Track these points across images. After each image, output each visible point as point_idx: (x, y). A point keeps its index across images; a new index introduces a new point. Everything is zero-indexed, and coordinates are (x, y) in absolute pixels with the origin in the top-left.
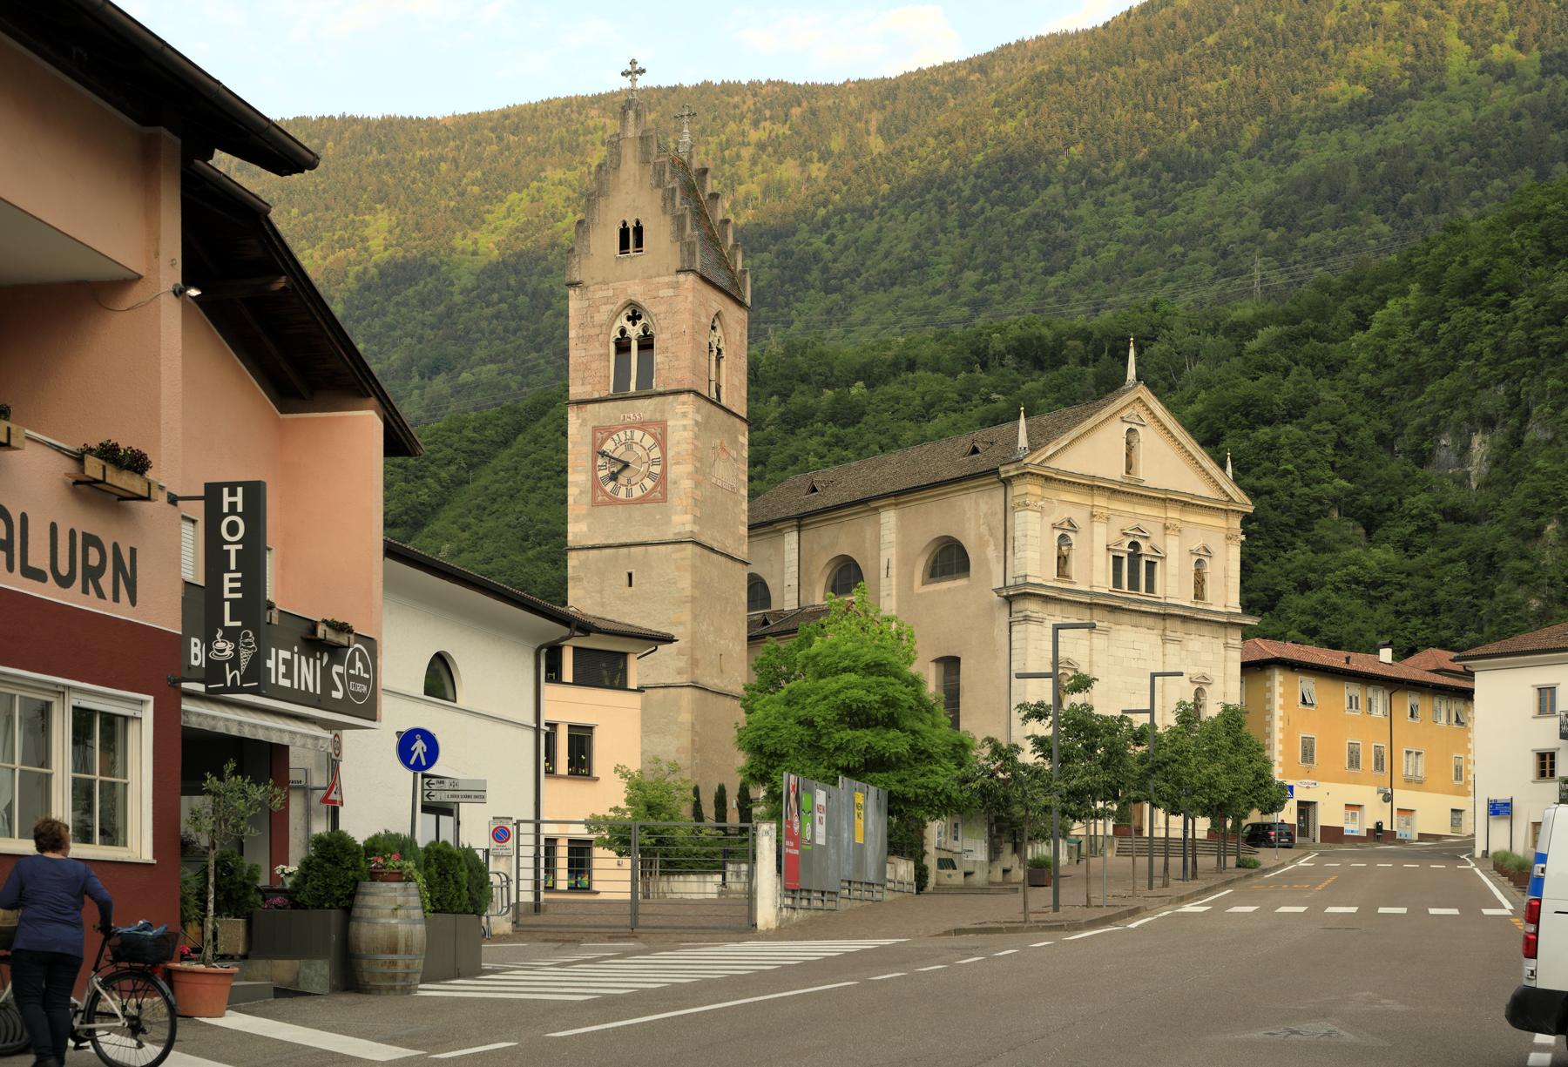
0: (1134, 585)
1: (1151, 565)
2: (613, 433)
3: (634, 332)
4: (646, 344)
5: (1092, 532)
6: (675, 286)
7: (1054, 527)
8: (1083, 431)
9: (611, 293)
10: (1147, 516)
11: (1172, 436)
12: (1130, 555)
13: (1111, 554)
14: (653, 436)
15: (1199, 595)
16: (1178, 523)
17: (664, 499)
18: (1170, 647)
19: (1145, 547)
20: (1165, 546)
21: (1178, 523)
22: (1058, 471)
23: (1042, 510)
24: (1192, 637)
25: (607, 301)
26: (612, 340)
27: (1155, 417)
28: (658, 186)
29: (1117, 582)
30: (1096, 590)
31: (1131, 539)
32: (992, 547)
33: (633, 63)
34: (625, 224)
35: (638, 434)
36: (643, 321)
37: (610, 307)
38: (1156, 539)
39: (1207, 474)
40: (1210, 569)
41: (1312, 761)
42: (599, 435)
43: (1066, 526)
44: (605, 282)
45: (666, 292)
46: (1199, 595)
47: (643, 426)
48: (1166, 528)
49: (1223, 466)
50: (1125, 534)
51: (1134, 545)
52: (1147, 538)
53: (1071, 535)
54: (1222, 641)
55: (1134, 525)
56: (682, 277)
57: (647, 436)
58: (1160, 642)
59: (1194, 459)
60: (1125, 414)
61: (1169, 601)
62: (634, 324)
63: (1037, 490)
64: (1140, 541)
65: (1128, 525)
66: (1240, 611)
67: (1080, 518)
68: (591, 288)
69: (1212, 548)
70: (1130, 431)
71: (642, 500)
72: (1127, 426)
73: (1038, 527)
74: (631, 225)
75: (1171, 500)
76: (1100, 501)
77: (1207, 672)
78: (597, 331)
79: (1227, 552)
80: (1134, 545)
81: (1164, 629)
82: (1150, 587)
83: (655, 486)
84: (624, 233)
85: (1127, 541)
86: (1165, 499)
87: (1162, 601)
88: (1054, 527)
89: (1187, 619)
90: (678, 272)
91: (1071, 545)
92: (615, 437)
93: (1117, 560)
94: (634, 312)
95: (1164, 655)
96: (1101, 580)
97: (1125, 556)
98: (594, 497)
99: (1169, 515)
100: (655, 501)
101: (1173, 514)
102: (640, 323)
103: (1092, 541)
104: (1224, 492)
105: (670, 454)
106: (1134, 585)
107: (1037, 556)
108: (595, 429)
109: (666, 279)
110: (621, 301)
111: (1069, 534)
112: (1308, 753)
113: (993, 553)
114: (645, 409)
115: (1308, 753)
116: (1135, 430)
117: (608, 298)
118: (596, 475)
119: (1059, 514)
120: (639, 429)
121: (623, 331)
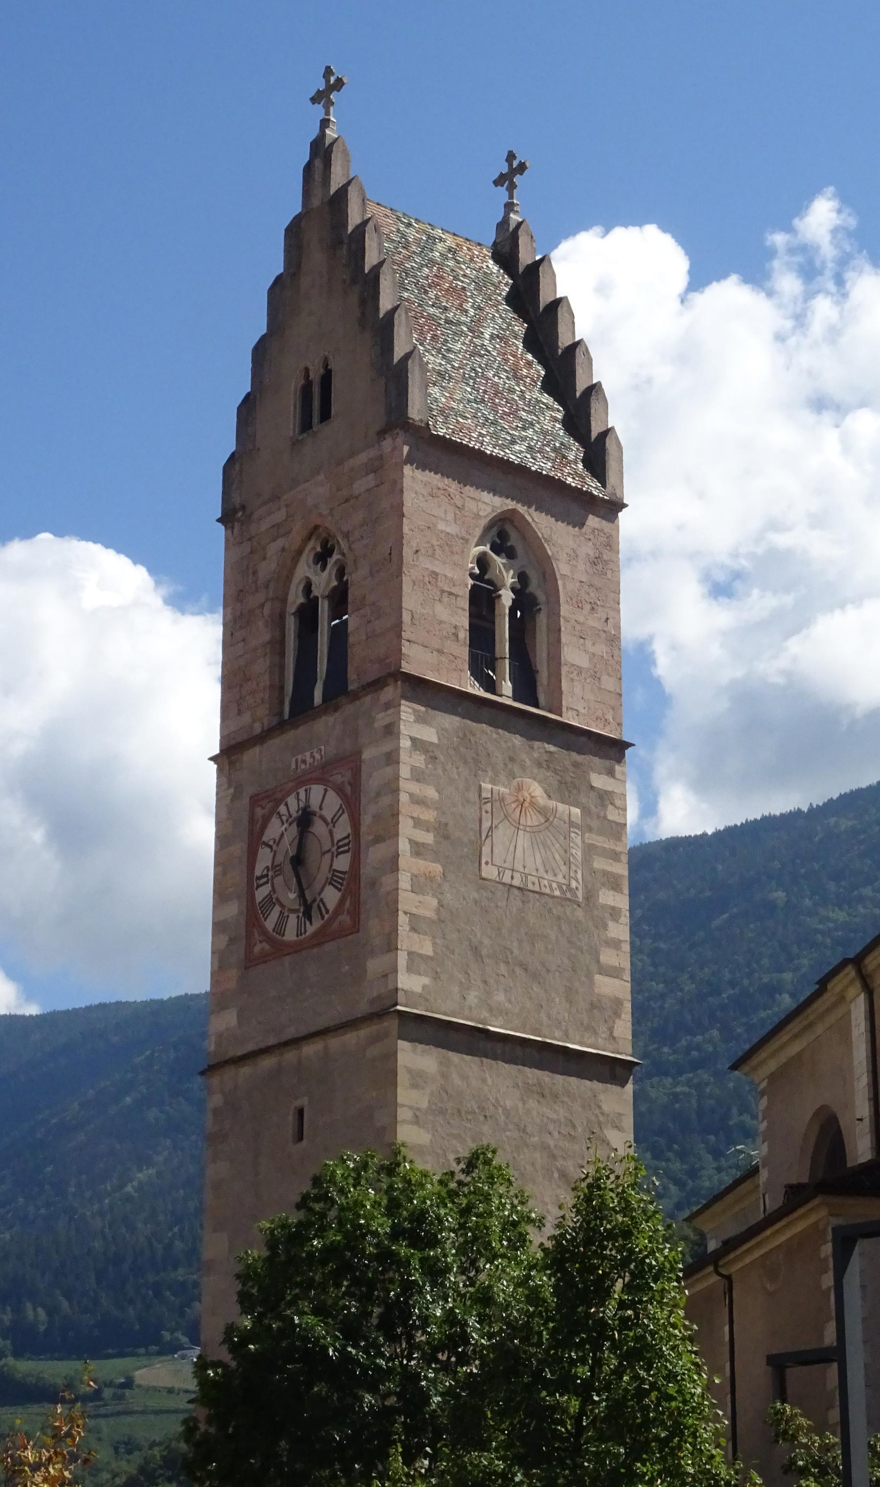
2: (278, 802)
9: (280, 516)
14: (339, 790)
17: (356, 927)
25: (279, 530)
34: (307, 370)
35: (317, 791)
36: (336, 557)
42: (259, 812)
56: (387, 444)
57: (331, 794)
68: (256, 516)
78: (261, 597)
90: (382, 433)
92: (282, 809)
94: (325, 544)
98: (249, 947)
100: (342, 933)
102: (331, 561)
105: (366, 820)
108: (255, 800)
109: (362, 458)
110: (298, 531)
117: (278, 526)
120: (319, 781)
121: (308, 587)
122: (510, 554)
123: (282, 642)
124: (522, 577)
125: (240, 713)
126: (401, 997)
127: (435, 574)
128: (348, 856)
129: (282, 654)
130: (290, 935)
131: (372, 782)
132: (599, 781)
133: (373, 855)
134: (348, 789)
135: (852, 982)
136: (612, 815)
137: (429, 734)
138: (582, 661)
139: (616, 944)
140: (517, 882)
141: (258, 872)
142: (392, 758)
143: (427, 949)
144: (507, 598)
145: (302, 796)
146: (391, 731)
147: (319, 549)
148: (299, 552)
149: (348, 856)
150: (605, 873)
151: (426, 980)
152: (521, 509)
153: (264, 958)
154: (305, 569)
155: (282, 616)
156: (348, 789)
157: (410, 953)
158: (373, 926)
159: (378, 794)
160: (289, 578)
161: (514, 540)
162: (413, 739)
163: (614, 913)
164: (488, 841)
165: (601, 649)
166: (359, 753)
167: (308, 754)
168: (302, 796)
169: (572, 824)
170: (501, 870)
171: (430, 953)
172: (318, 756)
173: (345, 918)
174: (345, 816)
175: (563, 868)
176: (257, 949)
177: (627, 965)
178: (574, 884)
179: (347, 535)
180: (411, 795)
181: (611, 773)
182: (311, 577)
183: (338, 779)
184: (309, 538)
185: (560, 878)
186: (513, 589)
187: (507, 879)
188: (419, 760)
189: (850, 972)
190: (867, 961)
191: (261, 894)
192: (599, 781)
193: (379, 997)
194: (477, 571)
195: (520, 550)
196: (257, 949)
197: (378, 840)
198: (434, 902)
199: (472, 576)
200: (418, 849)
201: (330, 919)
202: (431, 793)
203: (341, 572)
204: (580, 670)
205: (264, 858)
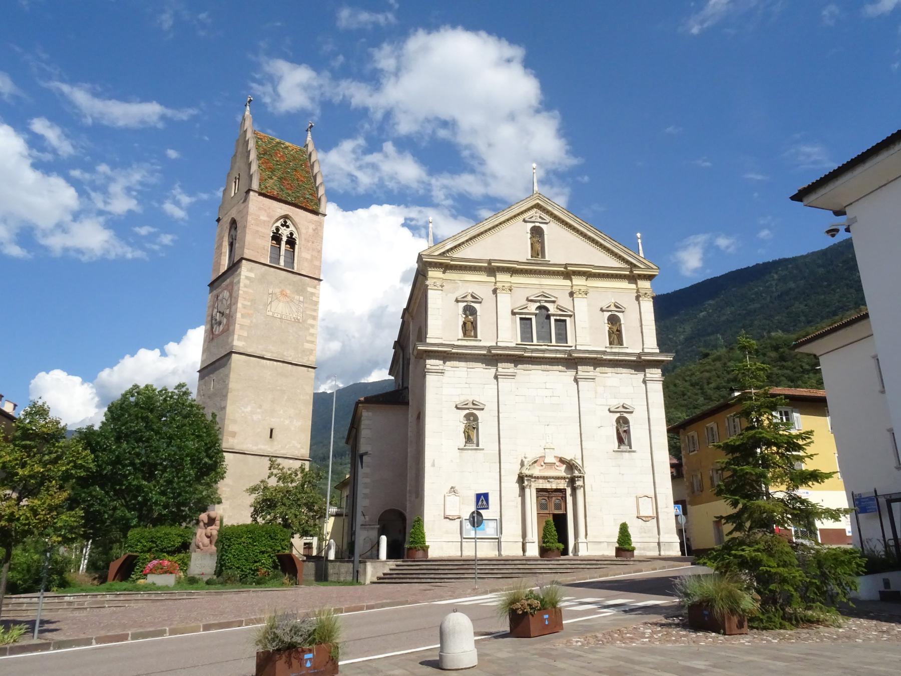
0: (545, 336)
1: (561, 323)
7: (457, 301)
8: (482, 230)
10: (556, 287)
13: (518, 317)
14: (229, 292)
17: (228, 330)
19: (552, 309)
29: (526, 334)
31: (538, 304)
50: (532, 301)
52: (554, 302)
53: (476, 306)
65: (532, 293)
66: (658, 351)
67: (484, 292)
71: (223, 332)
77: (628, 403)
82: (562, 336)
89: (597, 362)
91: (476, 313)
93: (525, 321)
101: (578, 281)
105: (233, 299)
122: (288, 227)
124: (292, 234)
126: (234, 347)
130: (217, 333)
131: (235, 288)
132: (310, 289)
133: (233, 308)
136: (314, 299)
137: (252, 275)
138: (308, 257)
140: (279, 316)
142: (239, 282)
143: (245, 334)
146: (240, 274)
150: (310, 315)
151: (244, 343)
157: (239, 335)
158: (231, 328)
161: (289, 223)
162: (246, 276)
164: (270, 305)
165: (315, 254)
169: (300, 301)
170: (274, 313)
175: (296, 314)
178: (299, 318)
180: (244, 292)
181: (315, 288)
185: (294, 316)
186: (288, 237)
187: (275, 315)
188: (248, 282)
192: (310, 289)
194: (275, 231)
197: (234, 304)
198: (249, 321)
199: (273, 233)
200: (245, 307)
202: (251, 291)
204: (307, 259)
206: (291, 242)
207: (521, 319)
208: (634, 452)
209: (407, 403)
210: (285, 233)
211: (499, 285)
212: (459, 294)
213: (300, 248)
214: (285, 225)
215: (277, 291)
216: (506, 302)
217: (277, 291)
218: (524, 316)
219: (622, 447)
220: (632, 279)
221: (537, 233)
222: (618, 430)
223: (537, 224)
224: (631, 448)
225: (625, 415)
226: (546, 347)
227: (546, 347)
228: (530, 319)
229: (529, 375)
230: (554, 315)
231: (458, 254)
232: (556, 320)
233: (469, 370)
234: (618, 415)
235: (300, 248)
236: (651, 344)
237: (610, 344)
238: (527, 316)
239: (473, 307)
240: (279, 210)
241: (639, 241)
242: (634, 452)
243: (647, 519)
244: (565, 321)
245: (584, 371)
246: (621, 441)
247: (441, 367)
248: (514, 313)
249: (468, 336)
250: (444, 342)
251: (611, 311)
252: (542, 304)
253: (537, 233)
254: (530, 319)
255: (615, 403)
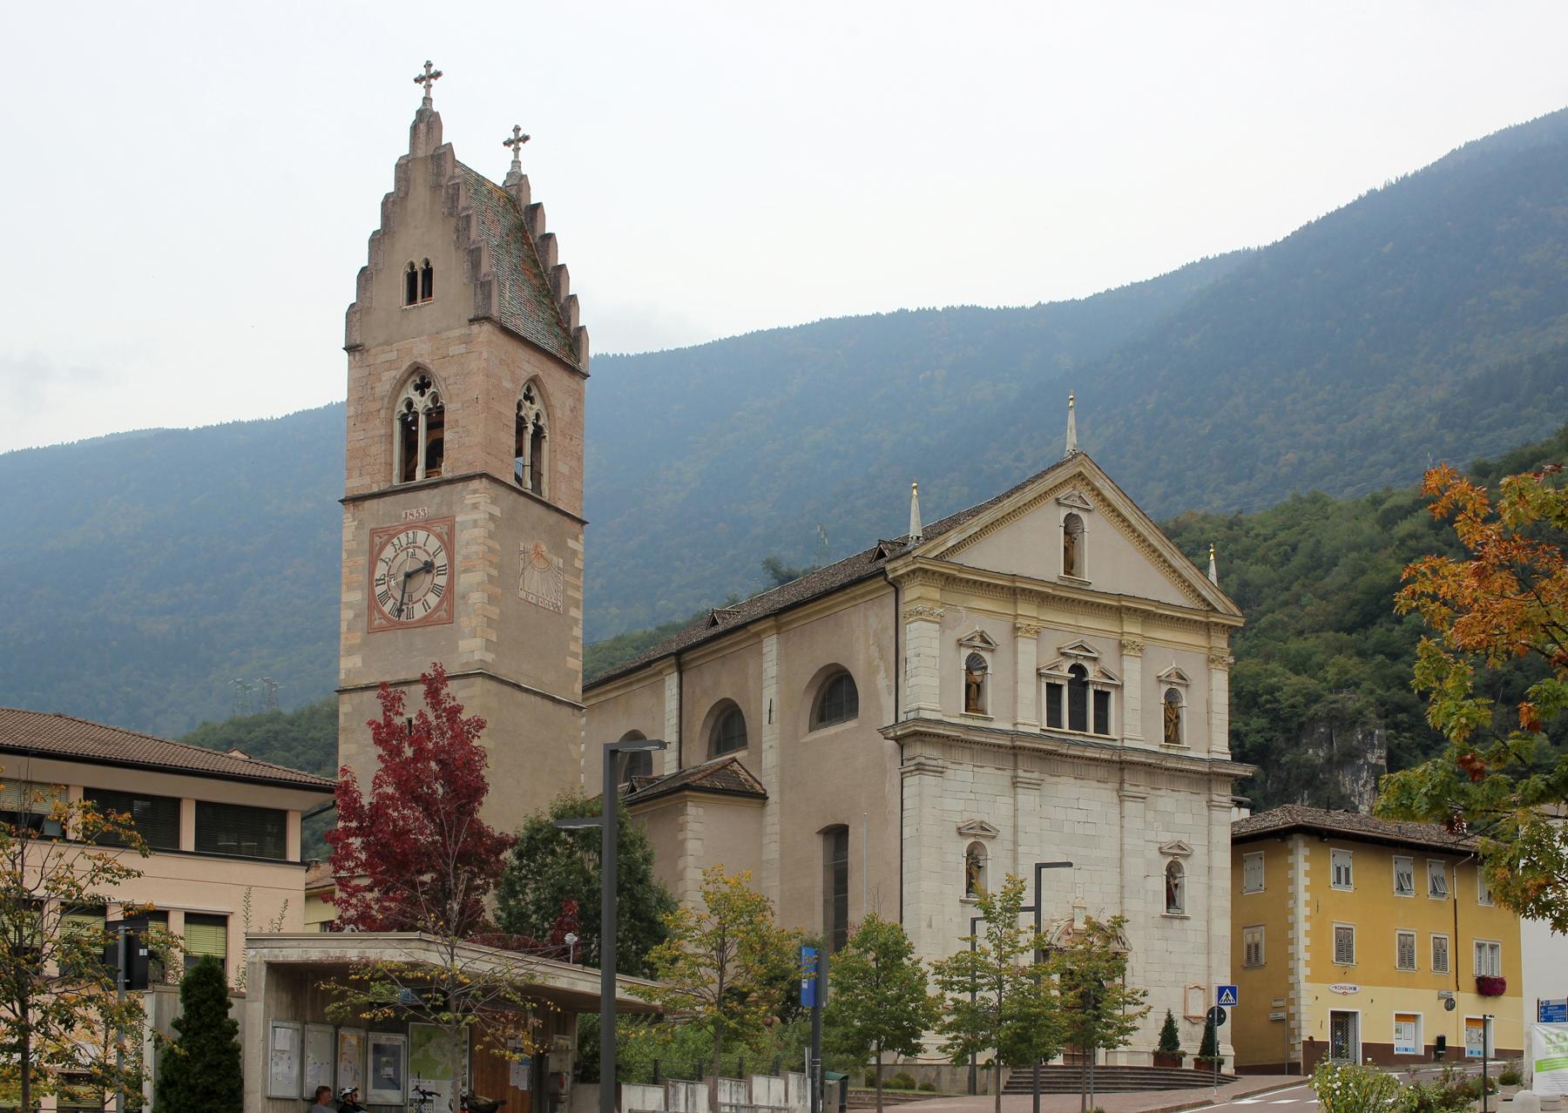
0: (1078, 722)
1: (1102, 698)
2: (393, 536)
3: (421, 403)
4: (436, 420)
5: (1015, 652)
6: (467, 340)
7: (960, 644)
9: (393, 355)
10: (1096, 632)
11: (1129, 526)
12: (1071, 682)
14: (439, 536)
15: (1172, 735)
16: (1138, 640)
17: (451, 619)
18: (1129, 806)
19: (1092, 673)
20: (1122, 670)
21: (1138, 640)
22: (961, 567)
23: (941, 622)
24: (1162, 792)
25: (390, 365)
26: (397, 416)
27: (1104, 499)
28: (451, 215)
29: (1054, 718)
30: (1021, 728)
32: (882, 674)
33: (428, 65)
34: (412, 265)
35: (421, 535)
36: (432, 389)
37: (393, 373)
38: (1109, 661)
39: (1180, 576)
40: (1189, 705)
41: (1350, 958)
42: (377, 540)
43: (977, 642)
44: (388, 343)
45: (456, 349)
46: (1172, 735)
47: (426, 524)
48: (1122, 646)
49: (1203, 569)
50: (1063, 654)
51: (1078, 670)
52: (1095, 659)
53: (986, 655)
54: (1203, 798)
55: (1076, 642)
58: (1116, 800)
59: (1160, 556)
60: (1061, 494)
61: (1127, 744)
62: (422, 394)
63: (935, 594)
64: (1086, 664)
65: (1068, 642)
66: (1229, 757)
67: (997, 631)
68: (373, 352)
69: (1188, 673)
70: (1069, 517)
71: (425, 622)
72: (1064, 512)
73: (936, 643)
74: (419, 267)
75: (1129, 609)
76: (1026, 609)
77: (1185, 840)
78: (378, 405)
79: (1210, 679)
80: (1078, 670)
81: (1122, 782)
83: (440, 603)
84: (412, 278)
85: (1067, 665)
86: (1120, 608)
87: (1118, 744)
88: (960, 644)
91: (985, 668)
92: (395, 541)
93: (1054, 690)
94: (423, 379)
95: (1122, 817)
96: (1030, 716)
97: (1065, 684)
98: (370, 621)
99: (1126, 629)
100: (440, 622)
101: (1132, 628)
102: (428, 392)
103: (1016, 663)
104: (1204, 600)
105: (458, 559)
106: (1078, 722)
107: (936, 682)
108: (373, 532)
111: (983, 654)
112: (1344, 950)
113: (883, 682)
114: (427, 503)
115: (1344, 950)
116: (1077, 517)
117: (391, 362)
118: (373, 591)
119: (969, 626)
120: (423, 528)
121: (410, 404)
122: (532, 400)
123: (392, 435)
125: (361, 475)
127: (500, 413)
128: (445, 577)
129: (392, 443)
134: (445, 537)
135: (669, 666)
139: (576, 639)
141: (377, 576)
143: (494, 639)
144: (531, 428)
145: (411, 535)
147: (418, 382)
148: (405, 382)
149: (445, 577)
151: (493, 656)
152: (541, 373)
153: (382, 629)
154: (411, 393)
155: (392, 420)
156: (445, 537)
159: (468, 544)
160: (397, 396)
163: (576, 621)
166: (454, 517)
167: (415, 510)
168: (411, 535)
171: (495, 640)
172: (422, 513)
173: (443, 614)
174: (443, 553)
176: (376, 623)
177: (581, 651)
179: (445, 380)
182: (413, 398)
183: (438, 530)
184: (412, 373)
189: (673, 660)
190: (685, 655)
191: (379, 590)
193: (467, 663)
195: (537, 399)
196: (376, 623)
197: (466, 571)
201: (431, 613)
203: (435, 398)
205: (381, 569)
206: (538, 434)
207: (1048, 685)
208: (1187, 918)
209: (762, 797)
210: (529, 412)
211: (1021, 622)
212: (964, 632)
213: (553, 451)
214: (528, 397)
215: (530, 546)
216: (1029, 655)
217: (530, 546)
218: (1052, 681)
219: (1171, 910)
220: (1208, 628)
221: (1071, 528)
222: (1168, 883)
223: (1075, 511)
224: (1183, 913)
225: (1181, 860)
226: (1081, 738)
227: (1081, 738)
228: (1060, 687)
229: (1056, 784)
230: (1094, 683)
231: (962, 558)
232: (1096, 692)
233: (975, 769)
234: (1170, 859)
235: (553, 451)
236: (1220, 747)
237: (1167, 739)
238: (1058, 682)
239: (981, 657)
240: (526, 366)
241: (1212, 557)
242: (1187, 918)
243: (1195, 1021)
244: (1108, 694)
245: (1136, 785)
246: (1171, 900)
247: (940, 762)
248: (1039, 675)
249: (973, 711)
250: (946, 719)
251: (1171, 683)
252: (1079, 662)
253: (1071, 528)
254: (1060, 687)
255: (1167, 838)
